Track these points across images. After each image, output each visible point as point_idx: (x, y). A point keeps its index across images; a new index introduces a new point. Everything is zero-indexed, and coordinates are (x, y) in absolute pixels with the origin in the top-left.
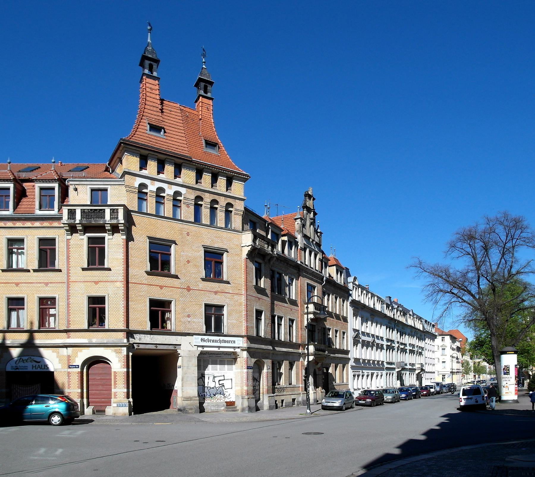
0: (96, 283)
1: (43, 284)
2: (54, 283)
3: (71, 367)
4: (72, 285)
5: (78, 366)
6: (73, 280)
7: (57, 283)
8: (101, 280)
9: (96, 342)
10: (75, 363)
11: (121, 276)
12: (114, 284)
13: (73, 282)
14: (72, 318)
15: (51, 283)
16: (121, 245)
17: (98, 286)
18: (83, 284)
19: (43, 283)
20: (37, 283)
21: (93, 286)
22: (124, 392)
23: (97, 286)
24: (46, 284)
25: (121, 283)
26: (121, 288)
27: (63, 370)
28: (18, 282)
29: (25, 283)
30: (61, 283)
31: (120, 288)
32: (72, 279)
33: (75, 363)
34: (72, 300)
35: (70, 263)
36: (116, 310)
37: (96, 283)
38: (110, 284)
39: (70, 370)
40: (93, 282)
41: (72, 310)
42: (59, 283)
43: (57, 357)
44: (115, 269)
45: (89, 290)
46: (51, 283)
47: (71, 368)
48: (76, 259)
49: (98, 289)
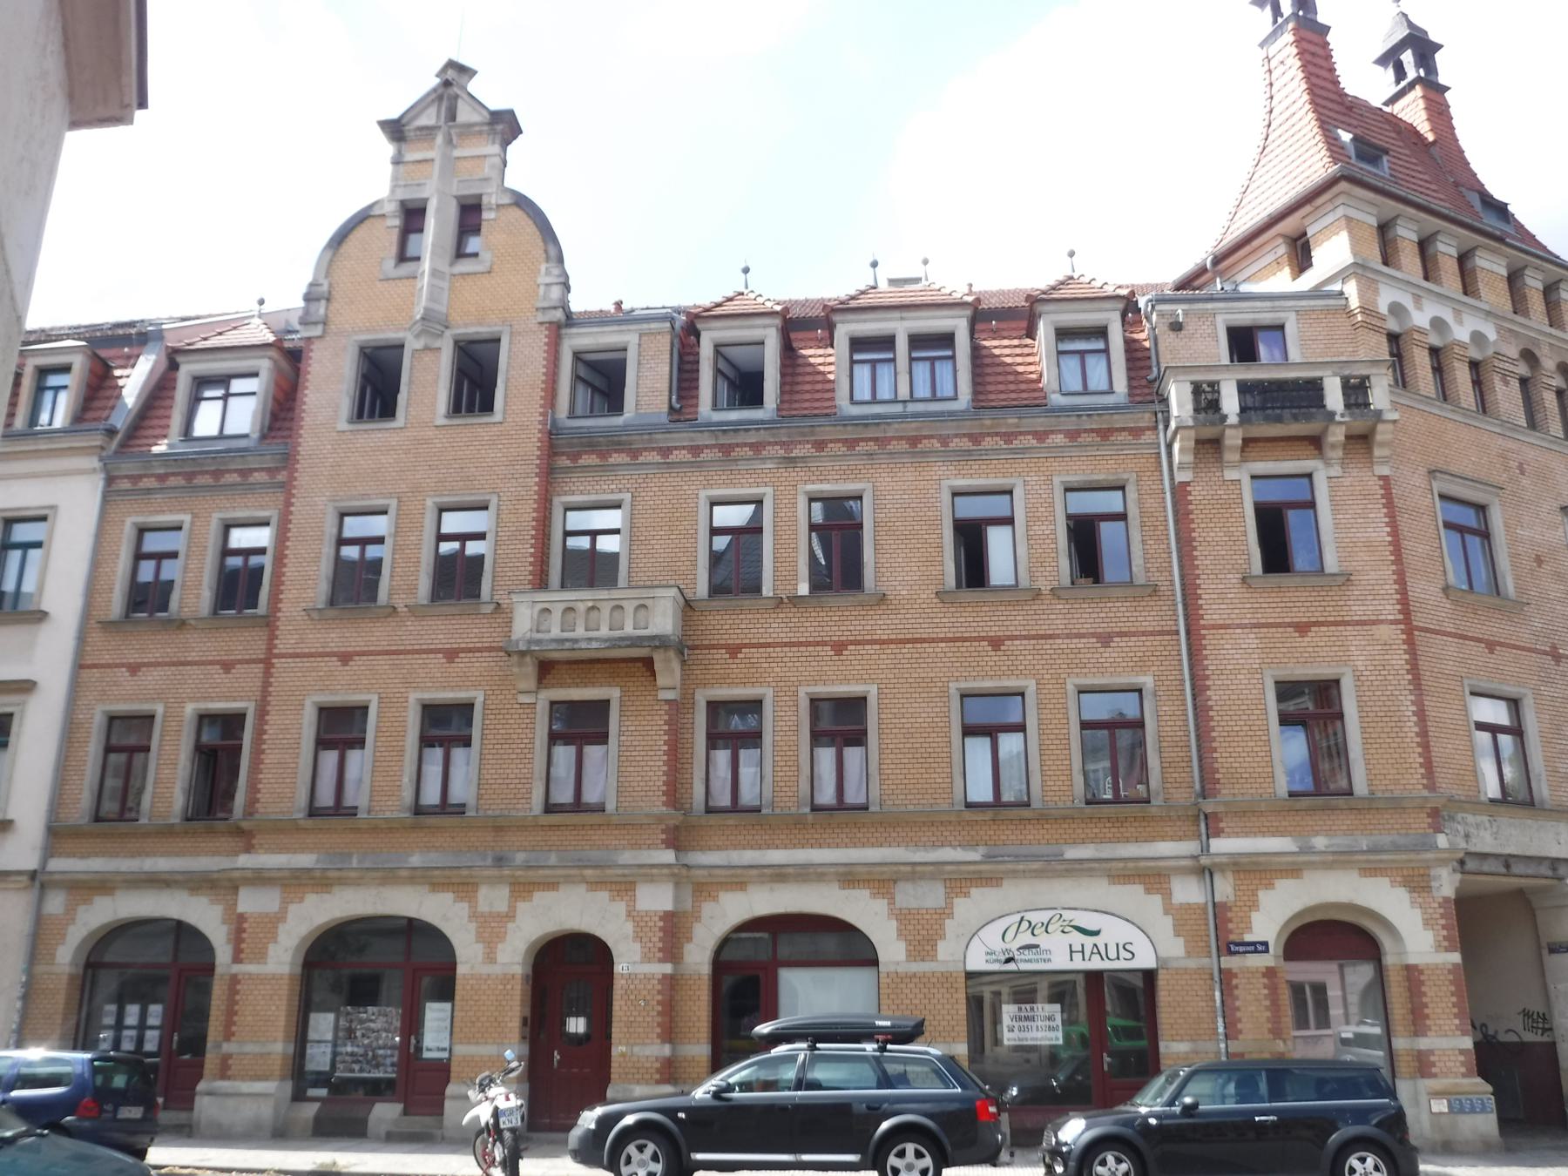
0: (1302, 628)
1: (1094, 640)
2: (1134, 634)
3: (1237, 948)
4: (1210, 640)
5: (1265, 944)
6: (1212, 622)
7: (1144, 634)
8: (1320, 619)
9: (1326, 847)
10: (1251, 932)
11: (1391, 602)
12: (1370, 633)
13: (1214, 627)
14: (1224, 760)
15: (1121, 634)
16: (1375, 497)
17: (1309, 639)
18: (1253, 636)
19: (1093, 635)
20: (1068, 636)
21: (1292, 640)
22: (1462, 1052)
23: (1306, 639)
24: (1103, 640)
25: (1393, 627)
26: (1396, 647)
27: (1192, 964)
28: (1001, 634)
29: (1026, 638)
30: (1161, 633)
31: (1394, 647)
32: (1211, 613)
33: (1251, 932)
34: (1218, 693)
35: (1196, 563)
36: (1390, 724)
37: (1302, 628)
38: (1356, 633)
39: (1229, 962)
40: (1289, 625)
41: (1221, 729)
42: (1152, 633)
43: (1166, 912)
44: (1366, 577)
45: (1278, 655)
46: (1121, 634)
47: (1238, 952)
48: (1216, 548)
49: (1311, 649)
